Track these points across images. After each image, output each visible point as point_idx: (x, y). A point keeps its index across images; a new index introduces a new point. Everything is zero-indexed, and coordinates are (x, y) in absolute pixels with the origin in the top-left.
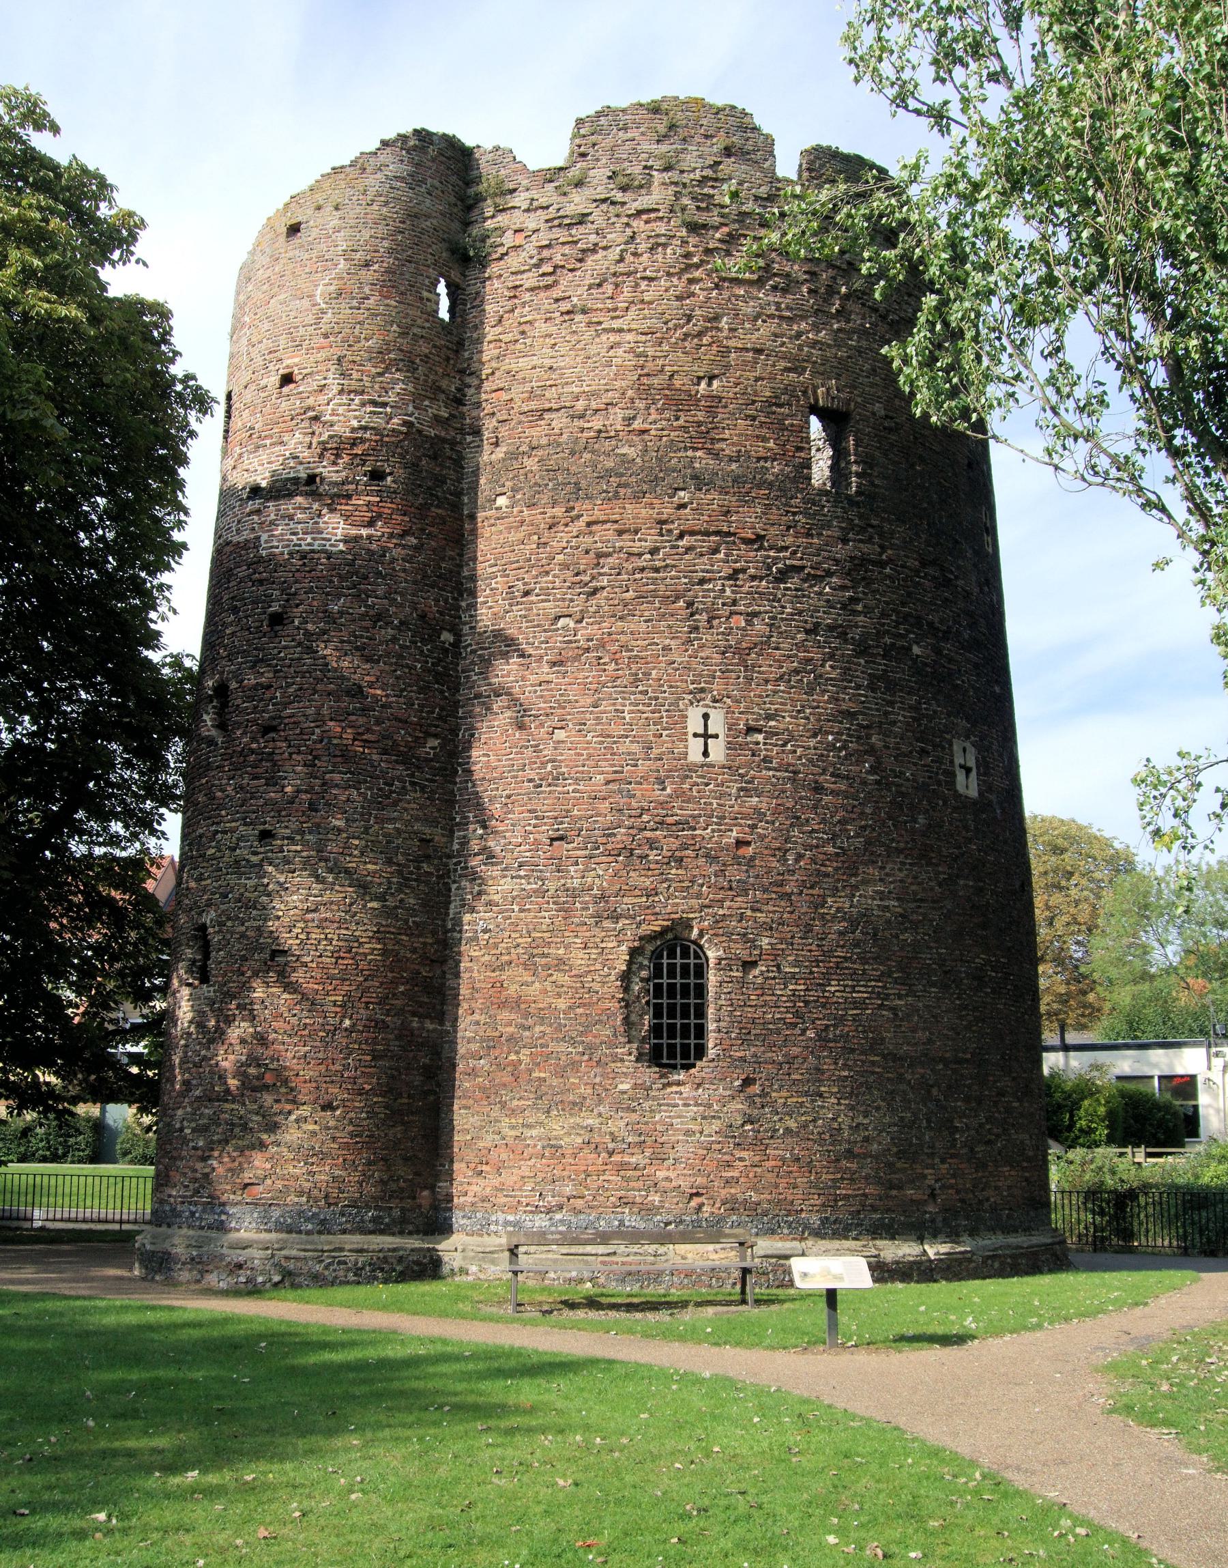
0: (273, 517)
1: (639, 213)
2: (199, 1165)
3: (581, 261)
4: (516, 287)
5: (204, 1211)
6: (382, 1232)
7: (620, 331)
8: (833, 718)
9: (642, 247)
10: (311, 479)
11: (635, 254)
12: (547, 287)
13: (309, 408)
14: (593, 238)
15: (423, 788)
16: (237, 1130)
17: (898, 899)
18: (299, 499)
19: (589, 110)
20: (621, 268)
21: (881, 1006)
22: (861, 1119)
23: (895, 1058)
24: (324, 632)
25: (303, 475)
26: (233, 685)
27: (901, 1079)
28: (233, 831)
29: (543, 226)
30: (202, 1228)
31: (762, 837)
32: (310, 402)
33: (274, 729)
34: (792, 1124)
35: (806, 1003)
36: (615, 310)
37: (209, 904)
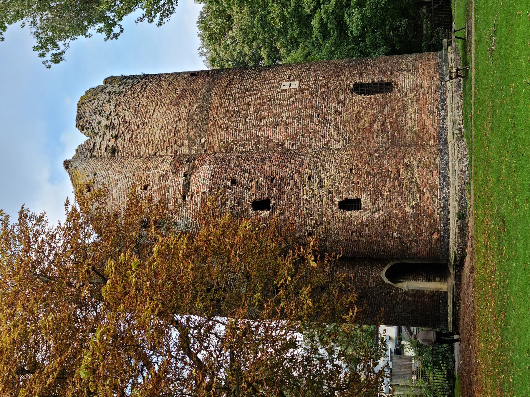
0: (196, 188)
1: (115, 107)
2: (426, 196)
3: (127, 122)
4: (129, 141)
5: (443, 192)
7: (154, 110)
9: (128, 106)
10: (185, 175)
11: (129, 108)
12: (133, 131)
13: (159, 179)
14: (120, 118)
16: (413, 180)
18: (192, 178)
19: (75, 123)
20: (133, 111)
24: (241, 167)
25: (184, 178)
26: (253, 198)
28: (307, 191)
29: (110, 134)
30: (449, 193)
32: (157, 178)
33: (273, 179)
36: (147, 112)
37: (332, 201)
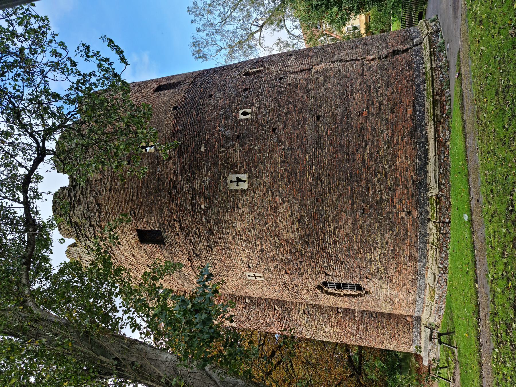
6: (420, 334)
8: (237, 244)
15: (290, 312)
17: (293, 224)
21: (334, 234)
22: (379, 245)
23: (353, 229)
27: (361, 227)
31: (283, 268)
34: (382, 268)
35: (337, 260)
